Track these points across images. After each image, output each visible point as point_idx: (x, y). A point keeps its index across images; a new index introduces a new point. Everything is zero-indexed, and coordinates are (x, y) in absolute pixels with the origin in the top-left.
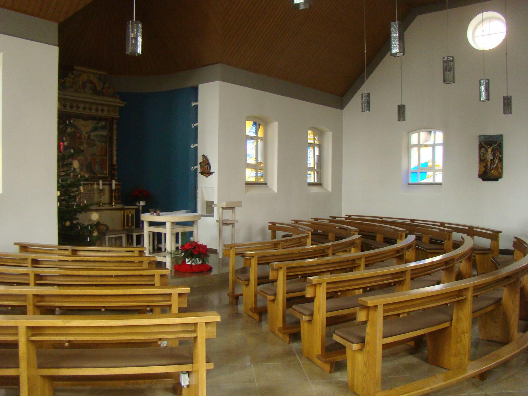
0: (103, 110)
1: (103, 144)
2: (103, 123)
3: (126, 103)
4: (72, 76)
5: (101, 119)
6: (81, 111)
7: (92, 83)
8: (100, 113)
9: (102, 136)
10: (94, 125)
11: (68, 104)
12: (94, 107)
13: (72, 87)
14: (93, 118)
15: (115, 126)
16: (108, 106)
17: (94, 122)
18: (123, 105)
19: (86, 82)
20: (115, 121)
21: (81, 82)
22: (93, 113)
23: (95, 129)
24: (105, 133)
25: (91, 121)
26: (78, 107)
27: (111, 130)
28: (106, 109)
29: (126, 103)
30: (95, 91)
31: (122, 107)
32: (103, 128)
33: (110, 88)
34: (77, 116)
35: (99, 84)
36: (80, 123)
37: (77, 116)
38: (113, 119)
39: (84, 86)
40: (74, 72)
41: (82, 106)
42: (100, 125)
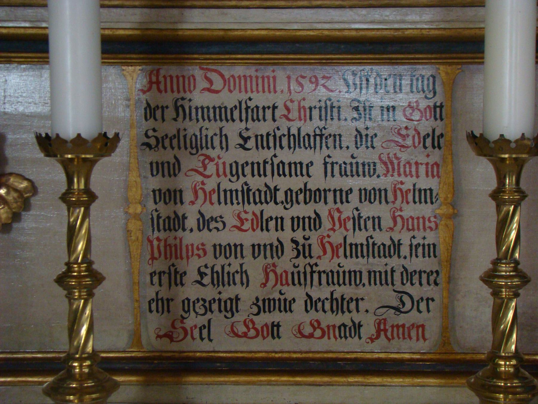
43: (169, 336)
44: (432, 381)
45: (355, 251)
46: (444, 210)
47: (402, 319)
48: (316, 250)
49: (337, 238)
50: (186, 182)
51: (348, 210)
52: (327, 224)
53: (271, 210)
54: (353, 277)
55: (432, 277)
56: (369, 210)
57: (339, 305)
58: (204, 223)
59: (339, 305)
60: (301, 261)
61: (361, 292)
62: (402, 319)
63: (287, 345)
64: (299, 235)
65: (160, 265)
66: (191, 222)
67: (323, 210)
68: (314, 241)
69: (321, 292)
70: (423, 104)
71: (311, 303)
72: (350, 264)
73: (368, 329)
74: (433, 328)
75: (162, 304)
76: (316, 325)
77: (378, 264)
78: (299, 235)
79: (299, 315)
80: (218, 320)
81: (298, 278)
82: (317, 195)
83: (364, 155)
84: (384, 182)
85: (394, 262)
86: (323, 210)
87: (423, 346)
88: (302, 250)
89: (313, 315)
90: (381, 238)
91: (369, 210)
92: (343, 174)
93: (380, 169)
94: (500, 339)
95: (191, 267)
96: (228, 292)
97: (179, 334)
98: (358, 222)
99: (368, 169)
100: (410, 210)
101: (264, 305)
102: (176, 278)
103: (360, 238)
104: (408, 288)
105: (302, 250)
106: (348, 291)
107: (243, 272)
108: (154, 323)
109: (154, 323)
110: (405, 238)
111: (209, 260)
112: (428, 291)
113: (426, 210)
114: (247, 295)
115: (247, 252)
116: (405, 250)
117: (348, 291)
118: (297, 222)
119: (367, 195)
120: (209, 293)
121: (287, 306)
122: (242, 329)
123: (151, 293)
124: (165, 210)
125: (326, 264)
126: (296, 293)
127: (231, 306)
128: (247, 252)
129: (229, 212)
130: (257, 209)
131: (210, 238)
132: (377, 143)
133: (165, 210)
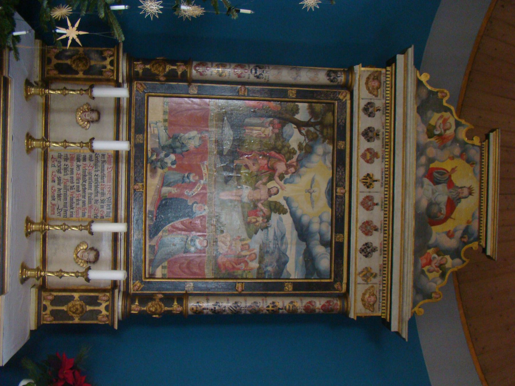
0: (367, 250)
1: (254, 265)
2: (324, 263)
3: (405, 335)
4: (462, 135)
5: (338, 252)
6: (361, 168)
7: (452, 205)
8: (358, 239)
9: (282, 263)
10: (315, 227)
11: (376, 122)
12: (377, 216)
13: (430, 133)
14: (339, 223)
15: (319, 303)
16: (387, 267)
17: (326, 229)
18: (394, 328)
19: (450, 184)
20: (337, 303)
21: (448, 166)
22: (360, 215)
23: (303, 233)
24: (294, 270)
25: (327, 214)
26: (370, 156)
27: (301, 288)
28: (375, 262)
29: (405, 335)
30: (427, 219)
31: (386, 324)
32: (309, 259)
33: (443, 276)
34: (340, 161)
35: (450, 235)
36: (318, 171)
37: (340, 161)
38: (345, 296)
39: (434, 176)
40: (476, 141)
41: (376, 169)
42: (319, 250)
43: (52, 158)
44: (42, 216)
45: (72, 199)
46: (80, 219)
47: (56, 209)
48: (72, 191)
49: (74, 195)
50: (88, 162)
51: (81, 198)
52: (78, 193)
53: (81, 181)
54: (66, 199)
55: (65, 216)
56: (81, 202)
57: (59, 196)
58: (78, 166)
59: (59, 196)
60: (69, 187)
61: (62, 200)
62: (56, 209)
63: (50, 184)
64: (75, 187)
65: (69, 156)
66: (78, 163)
67: (81, 193)
68: (74, 190)
69: (62, 192)
70: (104, 214)
71: (60, 190)
72: (68, 198)
73: (53, 202)
74: (54, 216)
75: (60, 156)
76: (55, 190)
77: (68, 205)
78: (75, 187)
79: (57, 187)
80: (57, 168)
81: (65, 187)
82: (84, 190)
83: (93, 202)
84: (87, 206)
85: (69, 208)
86: (81, 193)
87: (50, 214)
88: (72, 188)
89: (57, 190)
90: (74, 205)
91: (81, 202)
92: (89, 197)
93: (90, 205)
94: (53, 226)
95: (68, 163)
96: (62, 171)
97: (53, 160)
98: (78, 200)
99: (90, 202)
100: (80, 212)
101: (59, 179)
102: (66, 159)
103: (74, 200)
104: (63, 211)
105: (72, 188)
106: (62, 198)
107: (67, 174)
108: (56, 155)
109: (56, 155)
110: (74, 210)
111: (70, 167)
112: (62, 215)
113: (81, 214)
114: (62, 175)
115: (72, 176)
116: (72, 210)
117: (62, 198)
118: (78, 187)
119: (84, 202)
120: (62, 167)
121: (59, 184)
122: (54, 174)
123: (62, 154)
124: (81, 158)
125: (69, 193)
126: (62, 186)
127: (59, 171)
128: (72, 176)
129: (81, 172)
130: (81, 178)
131: (75, 167)
132: (96, 204)
133: (81, 158)
